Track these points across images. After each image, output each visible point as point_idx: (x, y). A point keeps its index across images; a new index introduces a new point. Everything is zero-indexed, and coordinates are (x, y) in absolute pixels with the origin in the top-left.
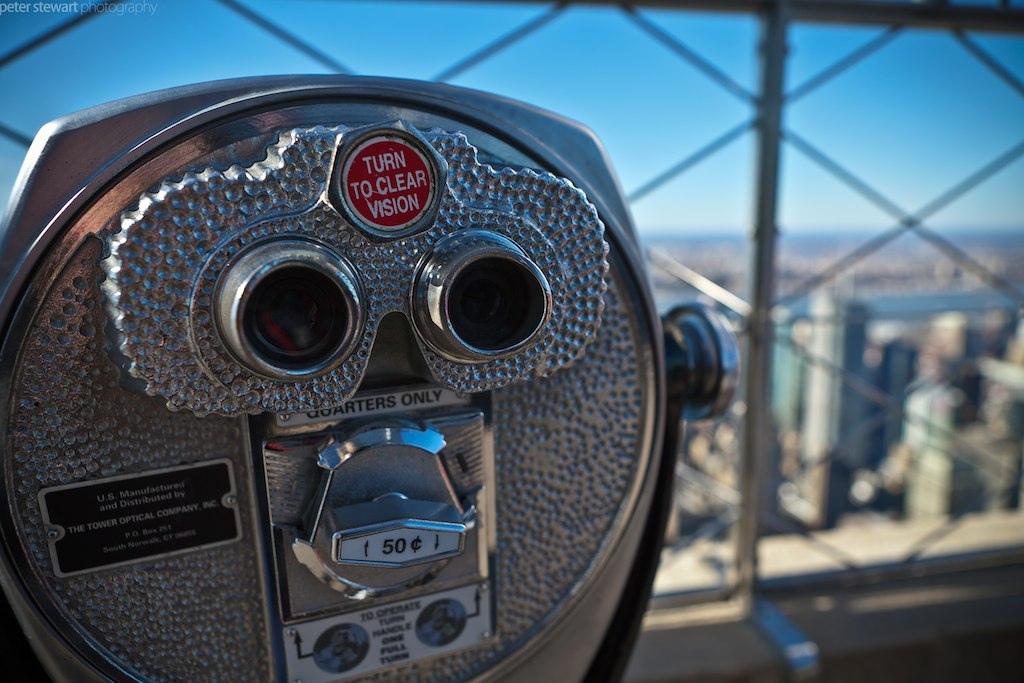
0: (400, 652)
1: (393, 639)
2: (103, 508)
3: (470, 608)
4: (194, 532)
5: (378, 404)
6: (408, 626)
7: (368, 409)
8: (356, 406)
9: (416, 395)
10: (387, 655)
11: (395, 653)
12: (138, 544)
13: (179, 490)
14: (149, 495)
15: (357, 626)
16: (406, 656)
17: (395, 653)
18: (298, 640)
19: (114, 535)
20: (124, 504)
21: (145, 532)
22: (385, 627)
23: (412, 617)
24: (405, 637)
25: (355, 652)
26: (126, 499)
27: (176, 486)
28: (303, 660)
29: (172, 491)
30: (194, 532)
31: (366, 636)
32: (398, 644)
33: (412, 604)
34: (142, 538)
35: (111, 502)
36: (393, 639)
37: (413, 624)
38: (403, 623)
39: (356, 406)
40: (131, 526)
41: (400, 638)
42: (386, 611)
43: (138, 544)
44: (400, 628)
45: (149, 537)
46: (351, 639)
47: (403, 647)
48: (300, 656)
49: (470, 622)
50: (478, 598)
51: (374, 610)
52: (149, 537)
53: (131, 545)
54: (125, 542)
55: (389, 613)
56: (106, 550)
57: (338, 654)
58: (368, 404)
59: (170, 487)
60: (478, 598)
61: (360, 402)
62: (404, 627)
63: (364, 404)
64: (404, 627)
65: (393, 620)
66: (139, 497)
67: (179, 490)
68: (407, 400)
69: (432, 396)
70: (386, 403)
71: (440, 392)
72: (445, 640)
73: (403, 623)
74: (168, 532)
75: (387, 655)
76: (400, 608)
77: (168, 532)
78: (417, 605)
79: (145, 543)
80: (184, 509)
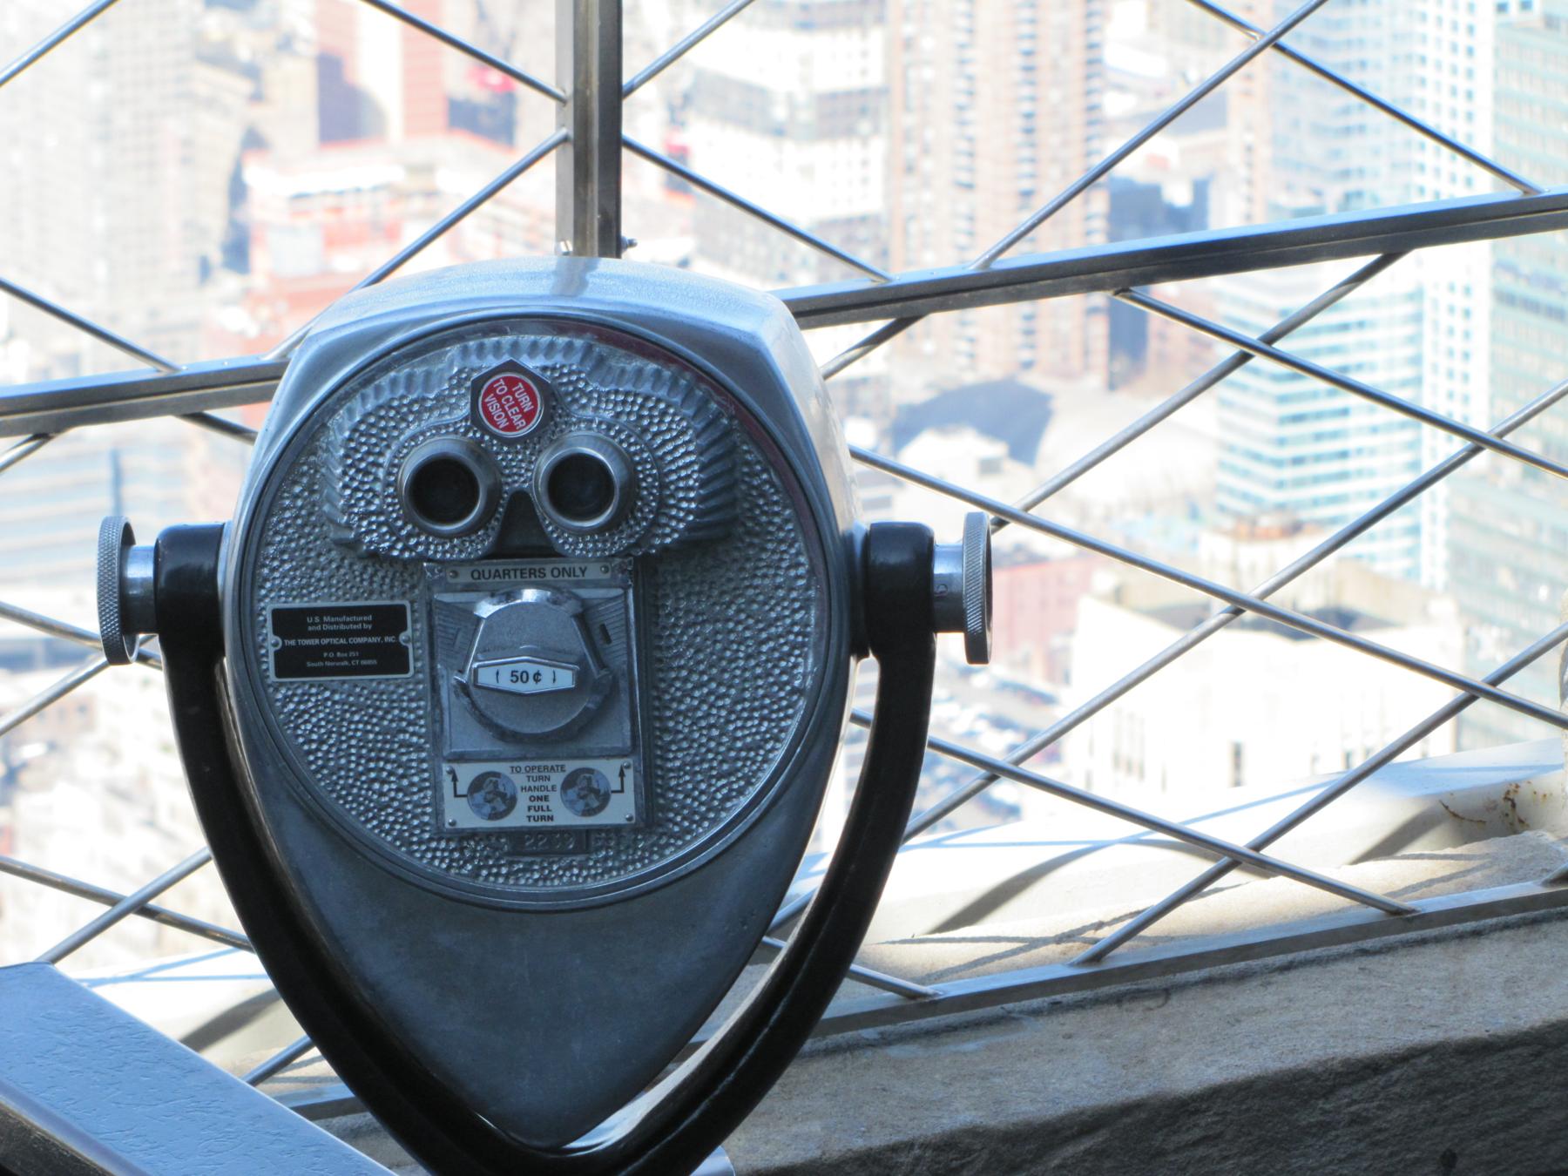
0: (546, 814)
1: (539, 798)
2: (310, 628)
3: (616, 785)
4: (374, 662)
5: (530, 574)
6: (553, 788)
7: (522, 577)
8: (512, 574)
9: (564, 569)
10: (532, 813)
11: (540, 813)
12: (332, 664)
13: (368, 622)
14: (346, 623)
15: (506, 777)
16: (551, 818)
17: (540, 813)
18: (455, 779)
19: (316, 653)
20: (326, 627)
21: (339, 654)
22: (532, 784)
23: (557, 779)
24: (550, 798)
25: (504, 802)
26: (327, 623)
27: (365, 618)
28: (459, 799)
29: (362, 622)
30: (374, 662)
31: (514, 788)
32: (544, 804)
33: (557, 766)
34: (336, 659)
35: (316, 624)
36: (539, 798)
37: (558, 788)
38: (549, 784)
39: (512, 574)
40: (330, 647)
41: (546, 798)
42: (533, 768)
43: (332, 664)
44: (546, 788)
45: (341, 659)
46: (501, 789)
47: (548, 810)
48: (456, 795)
49: (614, 797)
50: (622, 775)
51: (522, 764)
52: (341, 659)
53: (328, 664)
54: (324, 660)
55: (536, 771)
56: (309, 664)
57: (489, 802)
58: (522, 573)
59: (360, 619)
60: (622, 775)
61: (515, 570)
62: (550, 788)
63: (518, 573)
64: (550, 788)
65: (540, 778)
66: (337, 623)
67: (368, 622)
68: (556, 573)
69: (578, 572)
70: (537, 574)
71: (586, 568)
72: (589, 812)
73: (549, 784)
74: (355, 658)
75: (532, 813)
76: (546, 768)
77: (355, 658)
78: (562, 768)
79: (338, 664)
80: (370, 640)
